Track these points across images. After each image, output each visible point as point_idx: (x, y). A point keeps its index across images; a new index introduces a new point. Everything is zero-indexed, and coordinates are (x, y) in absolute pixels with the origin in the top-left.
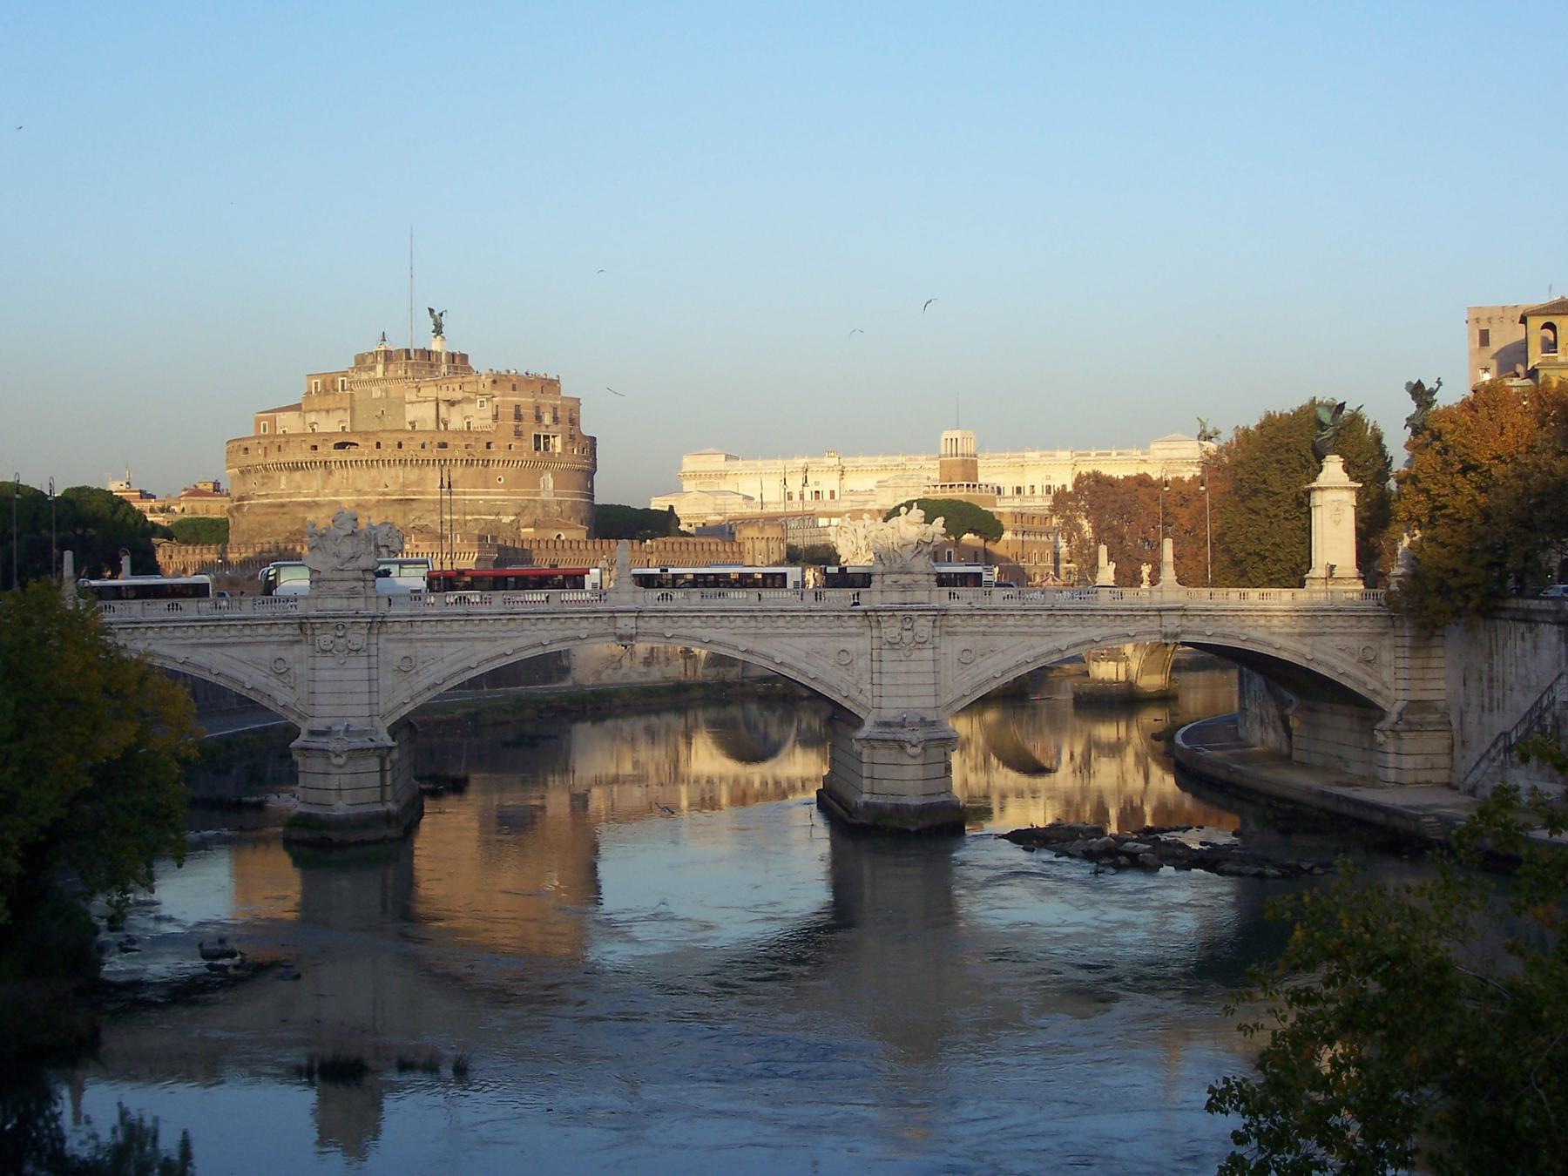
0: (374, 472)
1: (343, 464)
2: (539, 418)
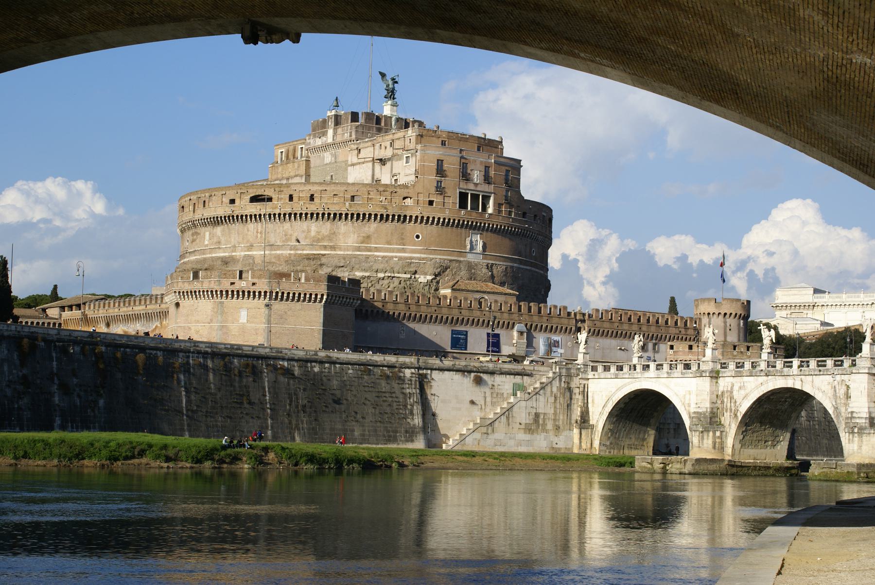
0: (287, 225)
1: (257, 218)
2: (465, 176)
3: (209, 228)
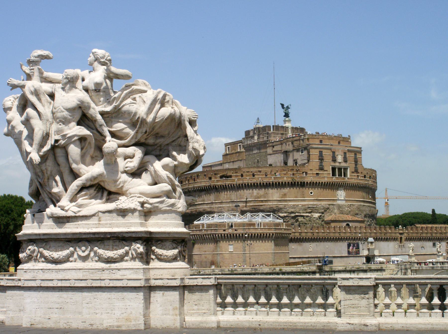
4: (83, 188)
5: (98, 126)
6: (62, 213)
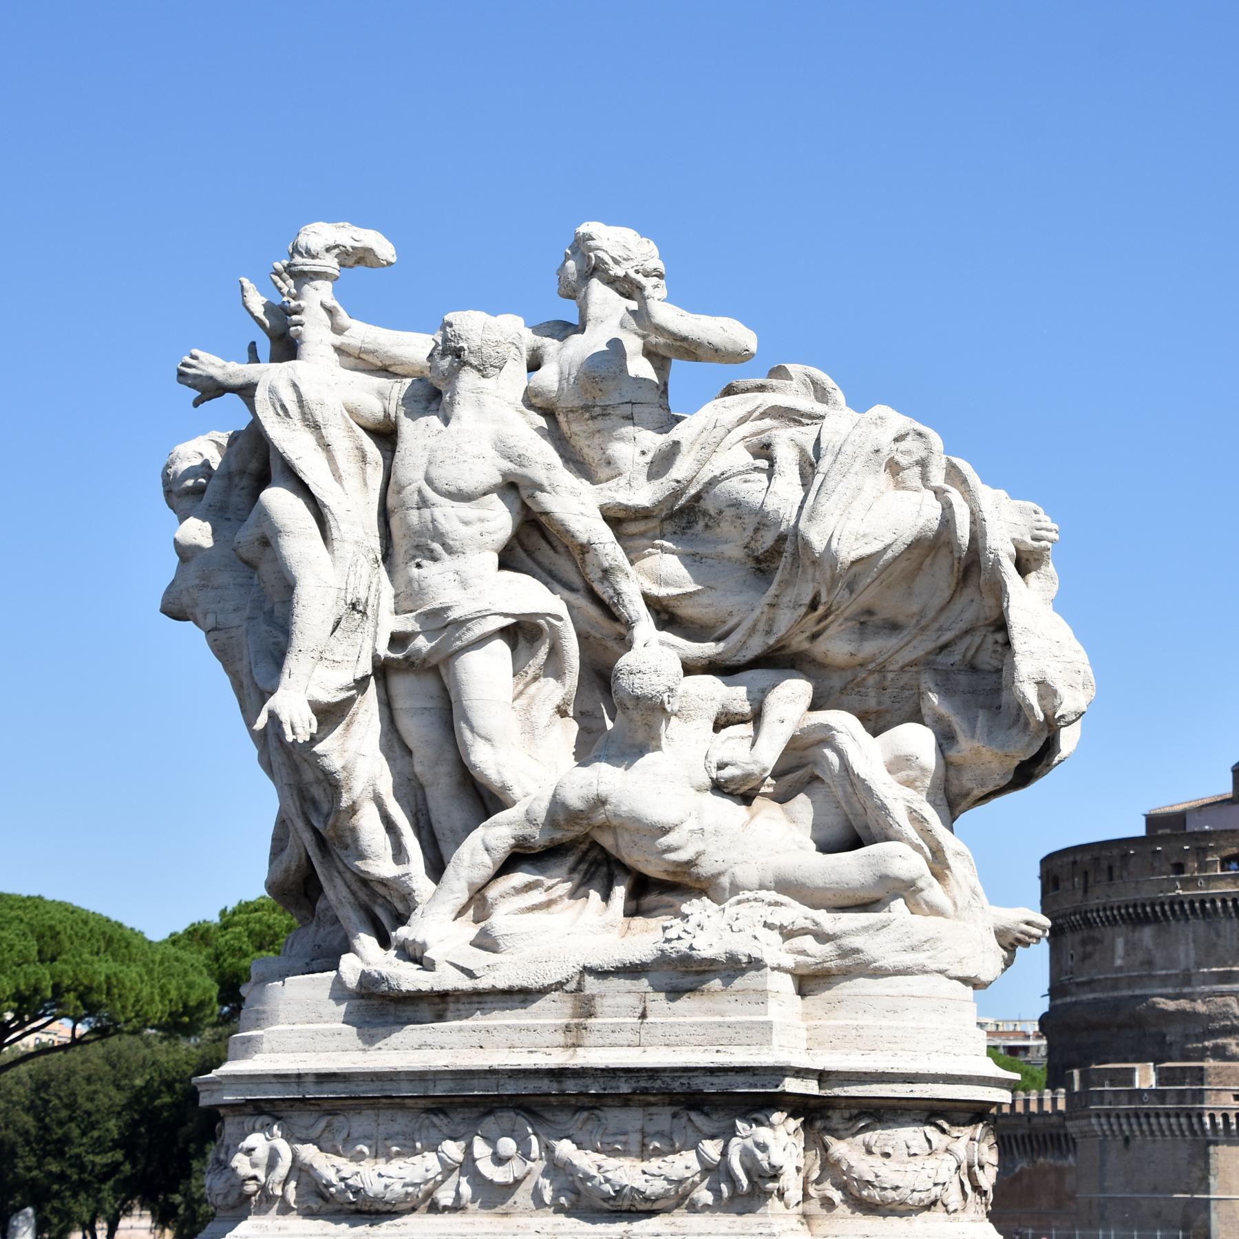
3: (1122, 929)
4: (517, 858)
5: (594, 575)
6: (409, 978)
